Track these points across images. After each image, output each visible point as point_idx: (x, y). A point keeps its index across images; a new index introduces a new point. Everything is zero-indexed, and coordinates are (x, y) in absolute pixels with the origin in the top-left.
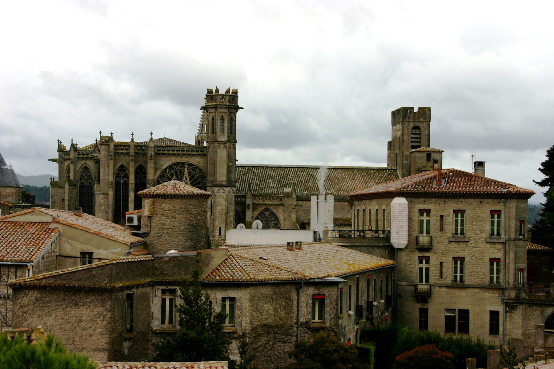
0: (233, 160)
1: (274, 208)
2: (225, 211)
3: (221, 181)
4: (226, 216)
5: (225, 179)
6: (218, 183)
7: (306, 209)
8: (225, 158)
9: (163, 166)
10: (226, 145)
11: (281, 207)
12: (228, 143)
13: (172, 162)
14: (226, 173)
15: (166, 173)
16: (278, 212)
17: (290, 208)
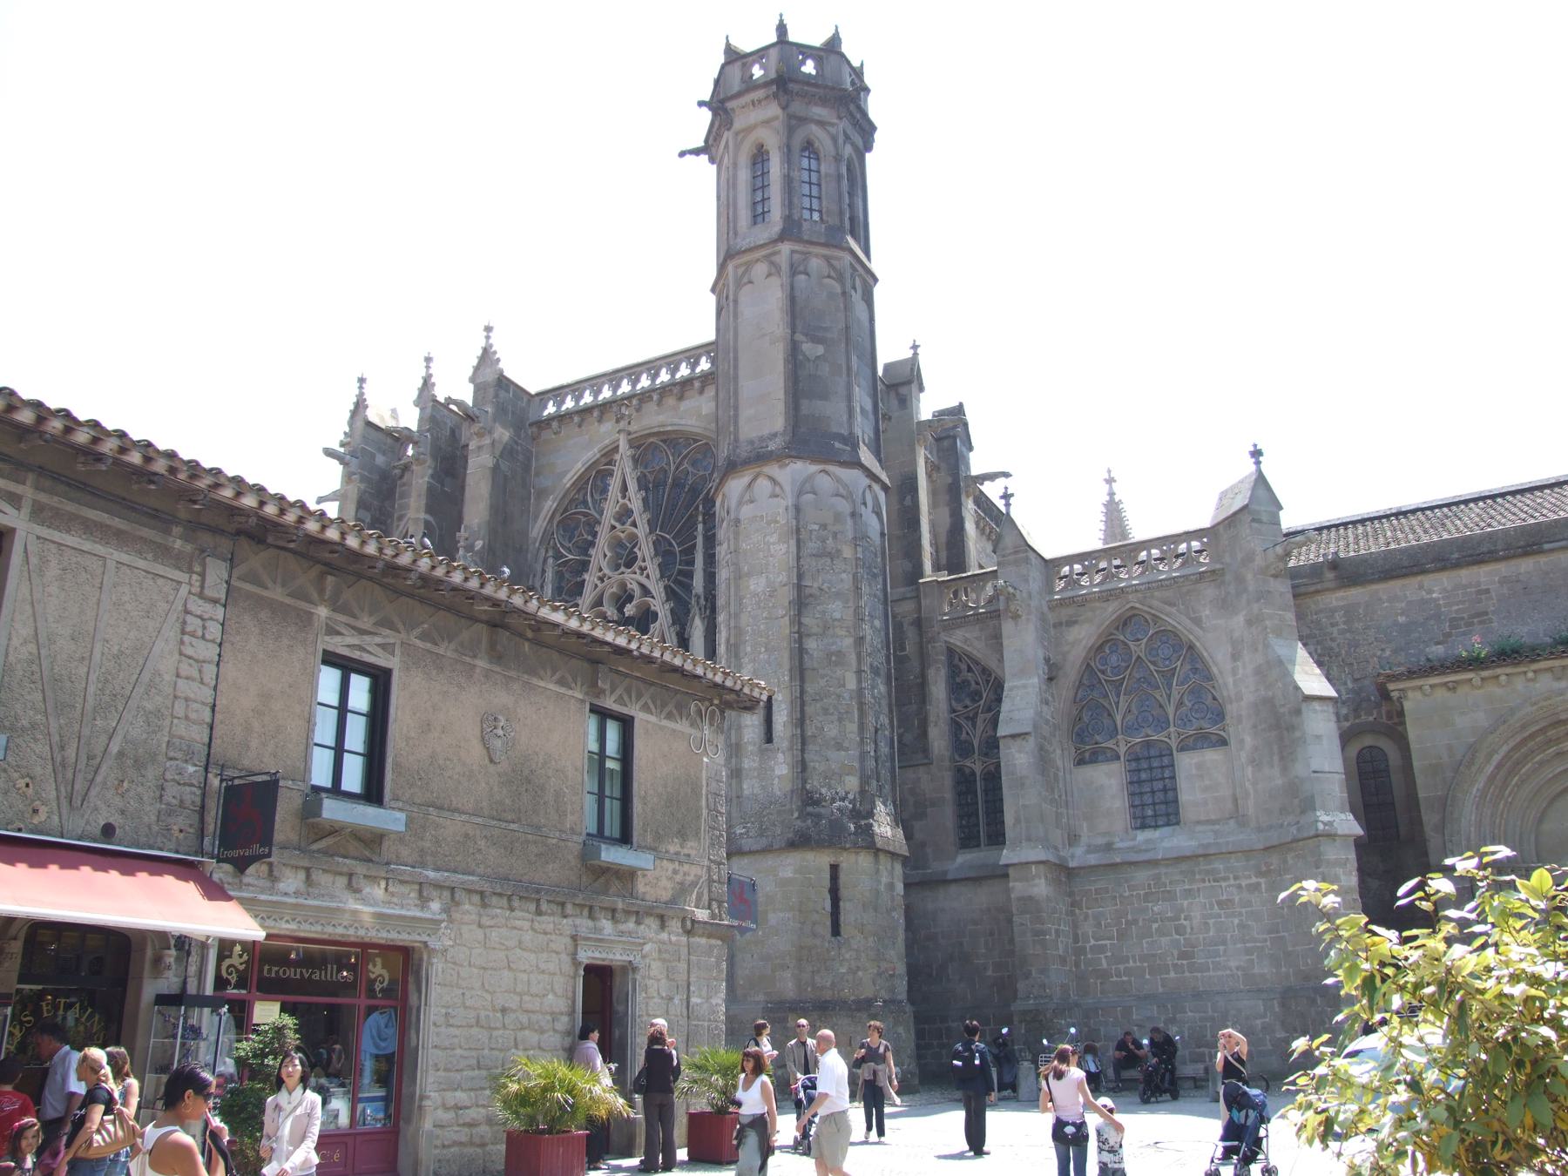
0: (826, 329)
1: (1172, 604)
2: (786, 595)
3: (762, 439)
4: (797, 620)
5: (779, 423)
6: (744, 451)
7: (1396, 623)
8: (777, 324)
9: (566, 472)
10: (776, 259)
11: (1209, 591)
12: (785, 248)
13: (600, 446)
14: (781, 395)
15: (585, 502)
16: (1197, 621)
17: (1249, 576)
